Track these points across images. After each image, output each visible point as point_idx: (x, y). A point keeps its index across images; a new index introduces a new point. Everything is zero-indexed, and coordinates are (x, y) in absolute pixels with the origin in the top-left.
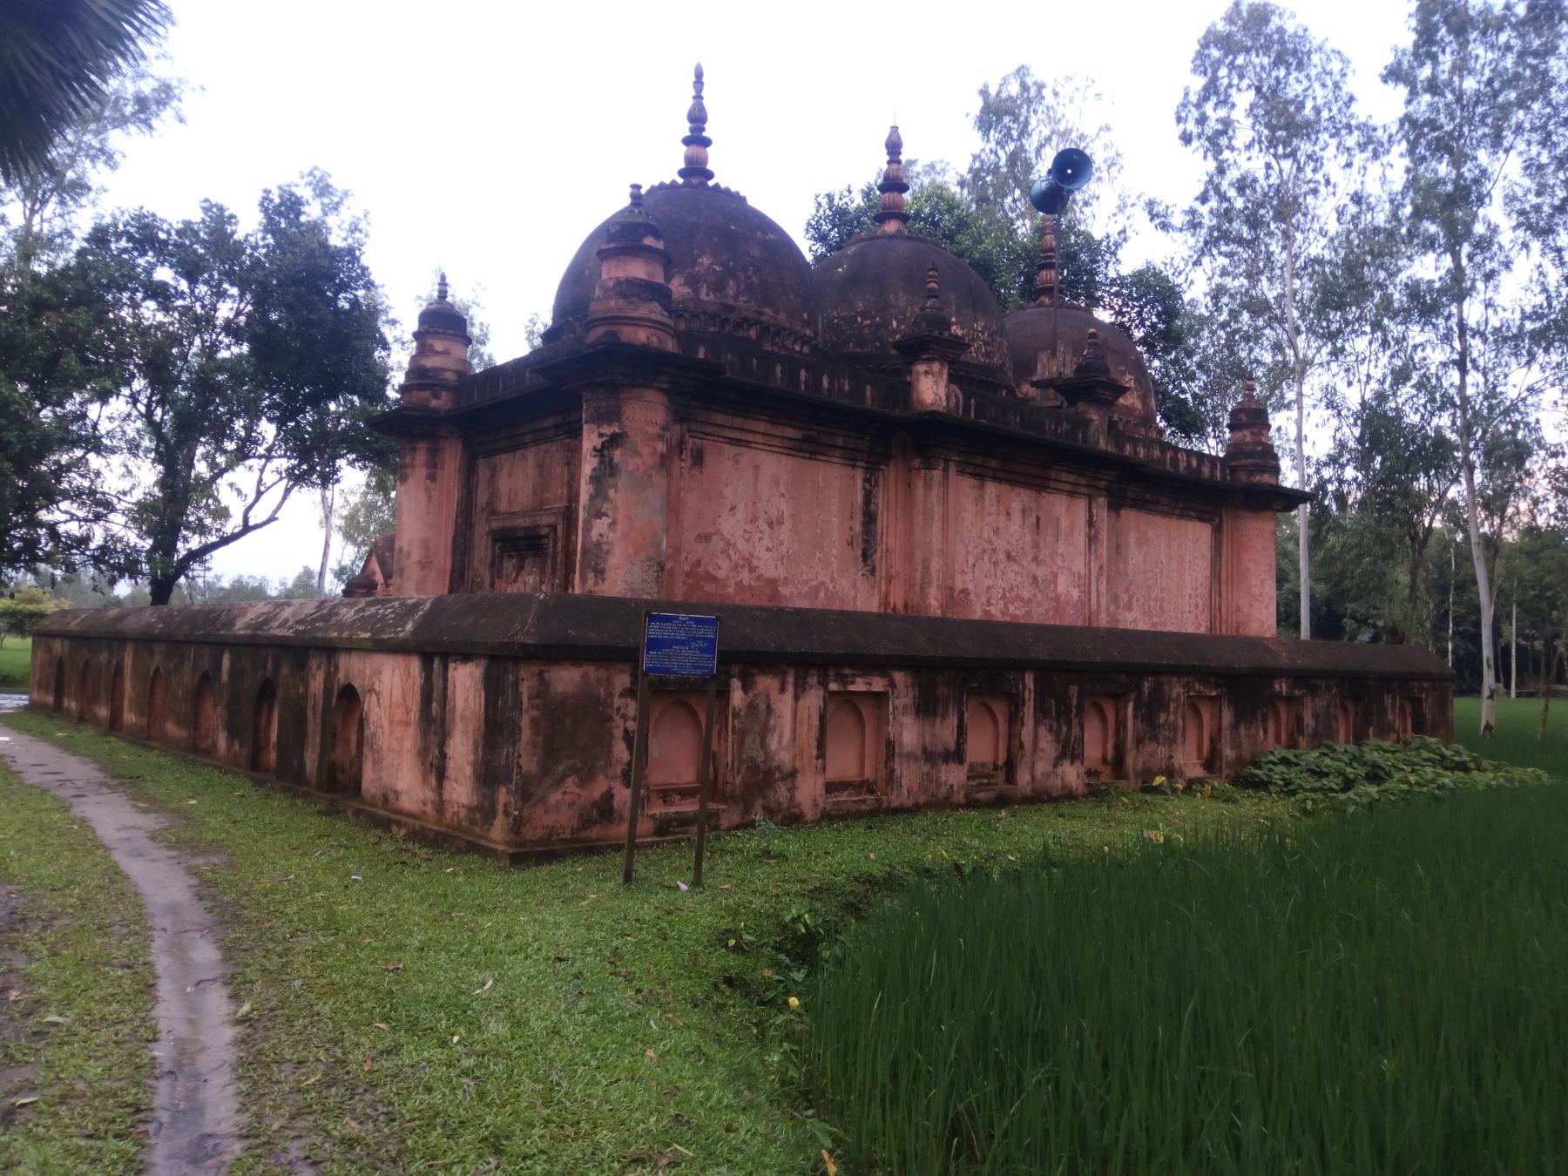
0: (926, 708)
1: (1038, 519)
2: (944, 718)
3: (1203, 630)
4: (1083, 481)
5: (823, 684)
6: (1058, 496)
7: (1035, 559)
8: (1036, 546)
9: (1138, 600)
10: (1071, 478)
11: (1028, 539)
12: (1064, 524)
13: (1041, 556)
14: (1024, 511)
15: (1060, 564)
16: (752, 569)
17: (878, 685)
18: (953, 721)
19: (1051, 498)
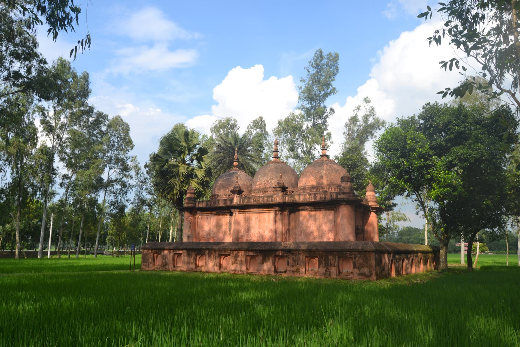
0: (189, 255)
1: (260, 220)
2: (191, 257)
3: (331, 240)
4: (270, 209)
5: (173, 252)
6: (265, 214)
7: (259, 228)
8: (260, 225)
9: (304, 233)
10: (267, 209)
11: (257, 224)
12: (267, 219)
13: (261, 227)
14: (256, 218)
15: (266, 228)
16: (210, 235)
17: (181, 252)
18: (193, 258)
19: (263, 214)
